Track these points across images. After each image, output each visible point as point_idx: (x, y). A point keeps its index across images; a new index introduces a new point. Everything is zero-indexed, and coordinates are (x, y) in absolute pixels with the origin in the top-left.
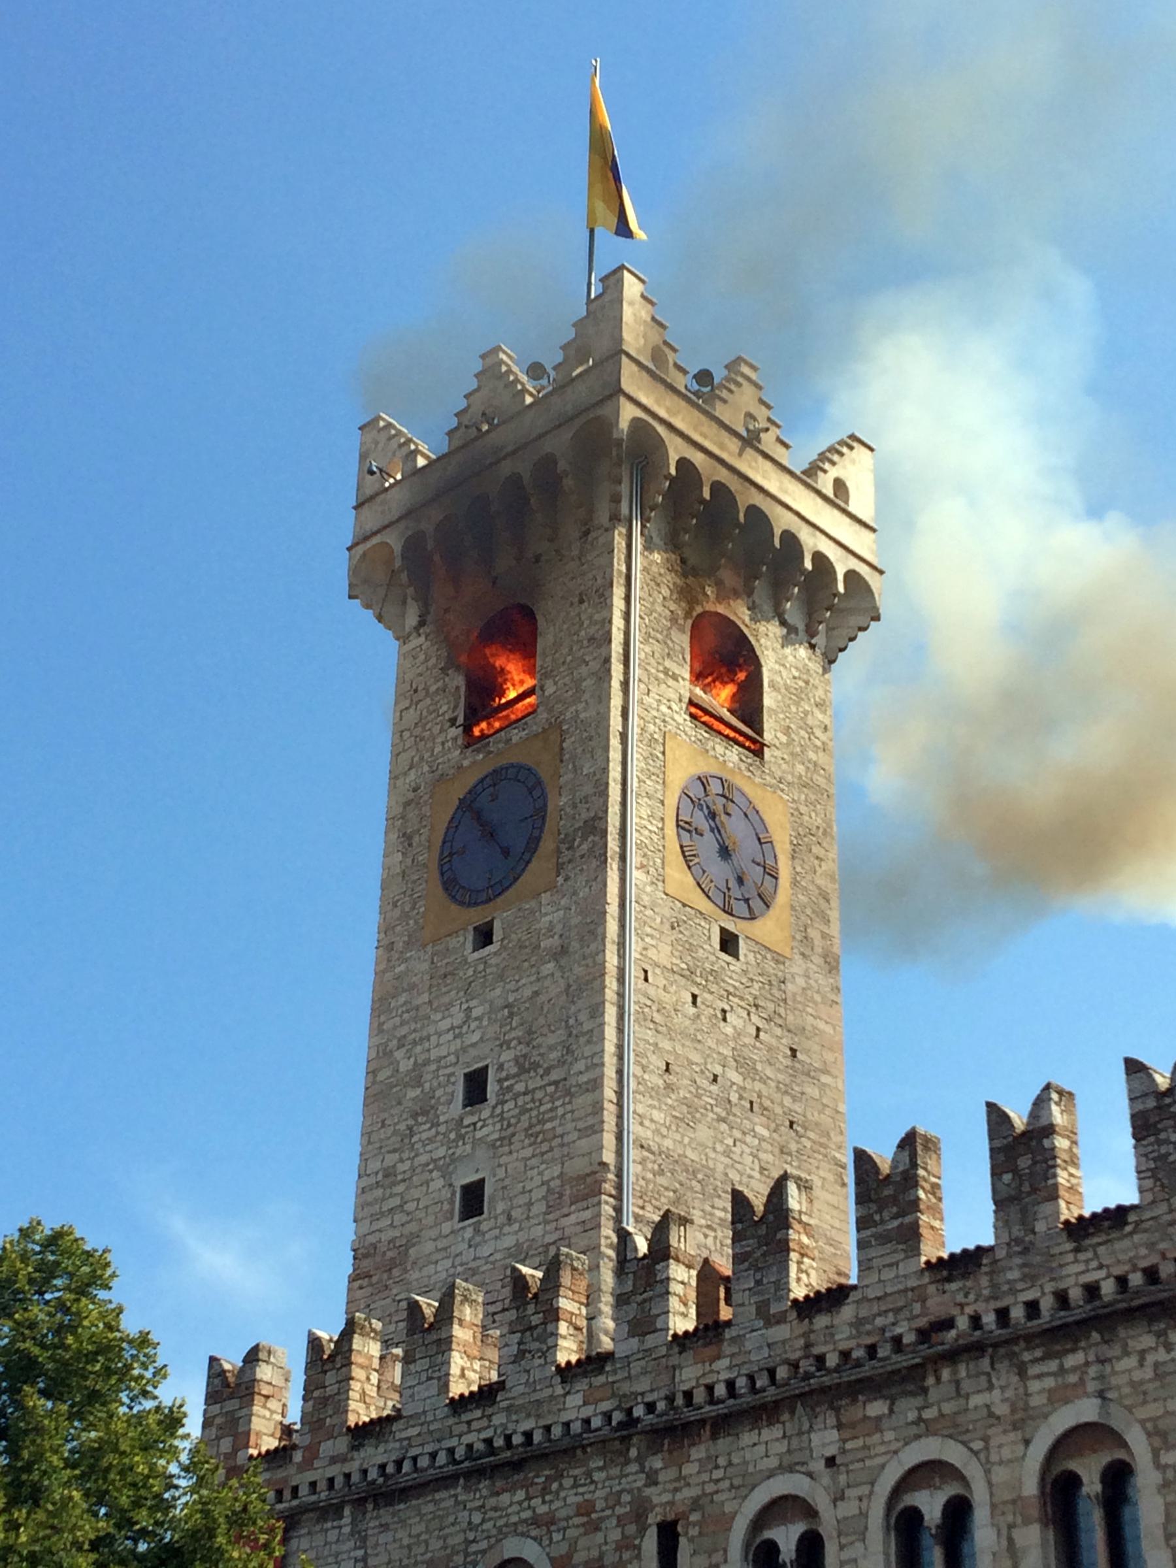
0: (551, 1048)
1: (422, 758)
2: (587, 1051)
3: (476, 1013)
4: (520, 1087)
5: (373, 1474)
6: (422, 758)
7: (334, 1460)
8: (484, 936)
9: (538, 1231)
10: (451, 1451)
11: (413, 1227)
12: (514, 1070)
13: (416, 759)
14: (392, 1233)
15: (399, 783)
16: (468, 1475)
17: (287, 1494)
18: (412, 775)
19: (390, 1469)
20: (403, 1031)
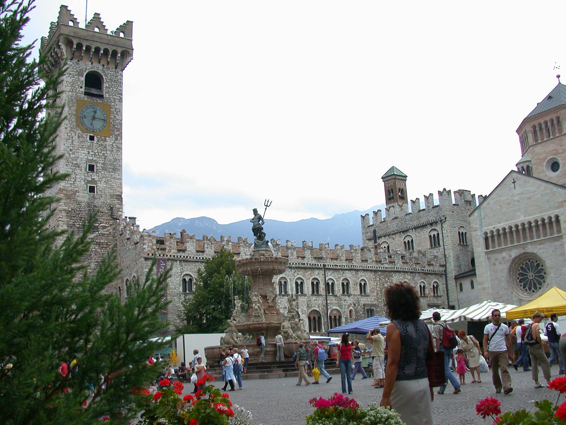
0: (110, 168)
1: (73, 91)
2: (118, 172)
3: (90, 153)
4: (103, 172)
5: (182, 257)
6: (73, 91)
7: (174, 253)
8: (92, 138)
9: (109, 201)
10: (197, 258)
11: (77, 189)
12: (101, 168)
13: (71, 90)
14: (71, 188)
15: (67, 92)
16: (201, 262)
17: (165, 256)
18: (70, 93)
19: (186, 257)
20: (72, 148)
